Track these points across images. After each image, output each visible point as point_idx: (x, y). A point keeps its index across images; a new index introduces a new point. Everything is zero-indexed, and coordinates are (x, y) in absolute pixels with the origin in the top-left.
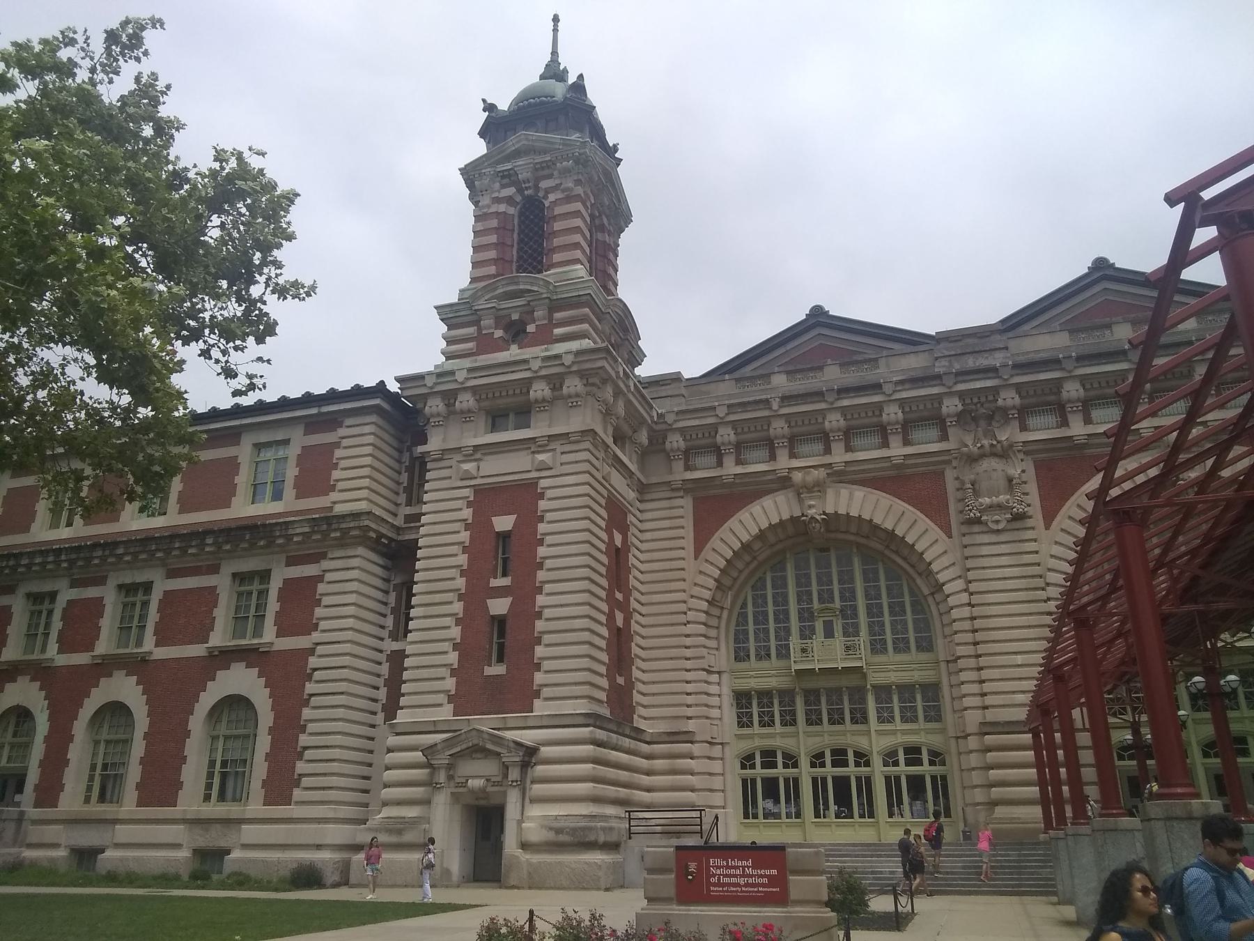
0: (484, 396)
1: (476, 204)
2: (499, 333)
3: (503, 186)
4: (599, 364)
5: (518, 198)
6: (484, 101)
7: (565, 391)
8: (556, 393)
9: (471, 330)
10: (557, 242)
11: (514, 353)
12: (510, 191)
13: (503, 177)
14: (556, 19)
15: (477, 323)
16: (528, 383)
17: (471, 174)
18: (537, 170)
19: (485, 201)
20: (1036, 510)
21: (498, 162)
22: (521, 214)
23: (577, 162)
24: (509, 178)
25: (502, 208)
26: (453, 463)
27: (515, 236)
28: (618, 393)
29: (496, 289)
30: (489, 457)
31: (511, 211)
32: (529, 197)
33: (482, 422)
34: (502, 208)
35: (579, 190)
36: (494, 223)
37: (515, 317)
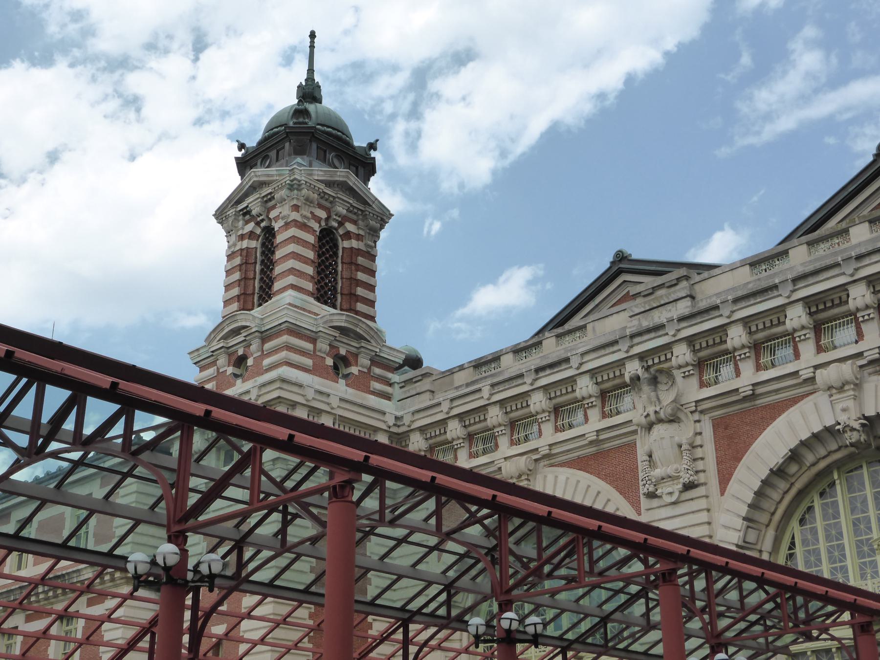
3: (247, 222)
4: (275, 395)
5: (258, 231)
12: (250, 226)
13: (244, 215)
14: (313, 35)
18: (266, 202)
20: (712, 477)
21: (239, 202)
23: (291, 188)
25: (245, 244)
27: (258, 267)
29: (223, 329)
31: (253, 244)
34: (245, 244)
35: (295, 216)
36: (238, 261)
37: (240, 352)
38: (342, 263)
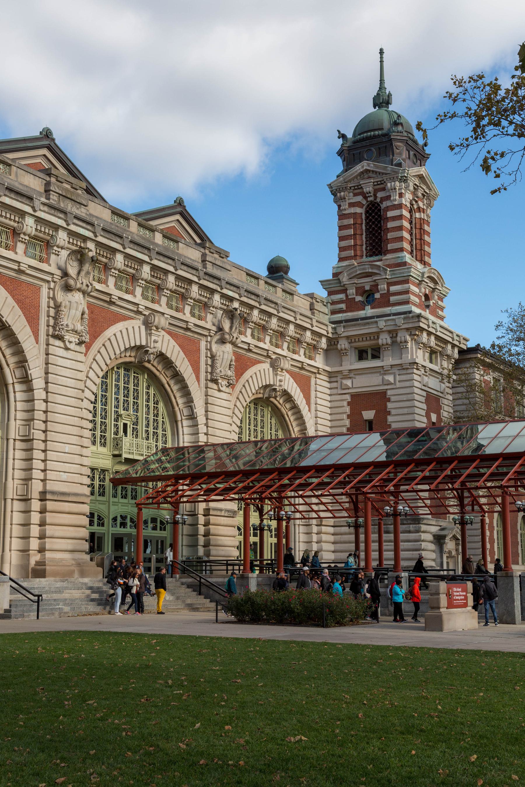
0: (353, 340)
1: (339, 206)
2: (359, 298)
3: (355, 195)
6: (339, 131)
7: (399, 339)
8: (394, 339)
9: (342, 296)
10: (390, 236)
11: (369, 311)
14: (381, 52)
15: (345, 291)
16: (376, 335)
17: (335, 191)
19: (345, 205)
22: (367, 212)
24: (358, 190)
26: (338, 379)
27: (364, 228)
28: (429, 334)
30: (357, 377)
32: (371, 201)
33: (353, 356)
37: (367, 288)
38: (415, 228)
